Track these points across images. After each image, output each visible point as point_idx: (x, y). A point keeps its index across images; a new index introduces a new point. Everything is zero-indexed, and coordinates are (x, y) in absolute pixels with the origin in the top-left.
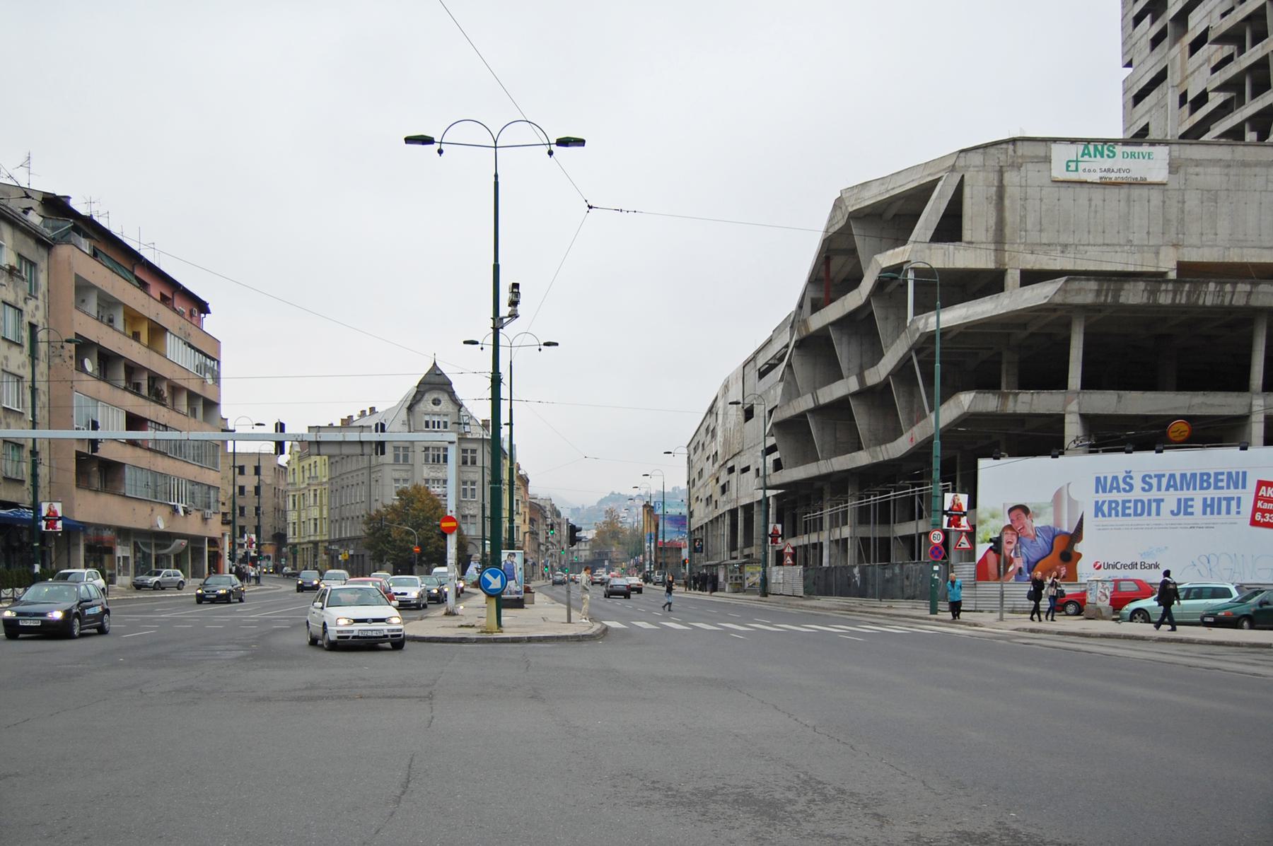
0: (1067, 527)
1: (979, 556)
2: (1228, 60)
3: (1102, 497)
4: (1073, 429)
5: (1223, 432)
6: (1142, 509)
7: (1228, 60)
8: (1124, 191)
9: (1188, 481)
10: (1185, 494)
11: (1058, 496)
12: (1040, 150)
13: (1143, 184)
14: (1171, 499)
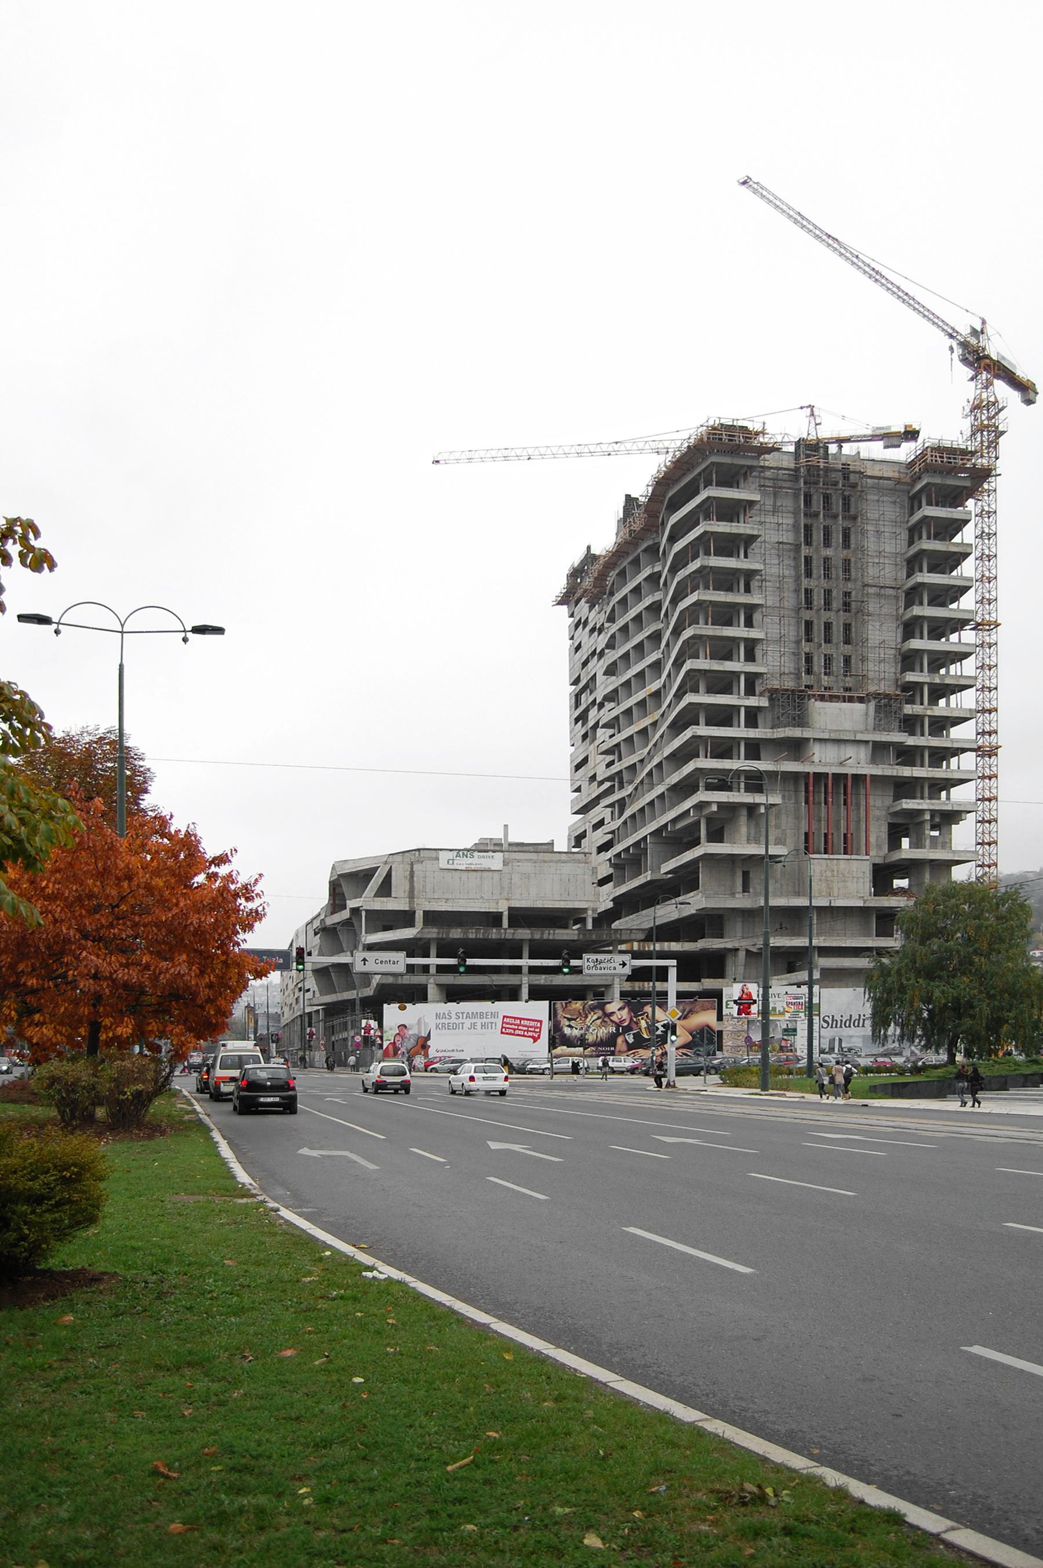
0: (424, 1034)
1: (385, 1047)
2: (612, 763)
3: (439, 1021)
4: (432, 991)
5: (512, 994)
6: (455, 1027)
7: (612, 763)
8: (479, 874)
9: (474, 1015)
10: (473, 1021)
11: (419, 1021)
12: (433, 854)
13: (489, 870)
14: (468, 1023)
